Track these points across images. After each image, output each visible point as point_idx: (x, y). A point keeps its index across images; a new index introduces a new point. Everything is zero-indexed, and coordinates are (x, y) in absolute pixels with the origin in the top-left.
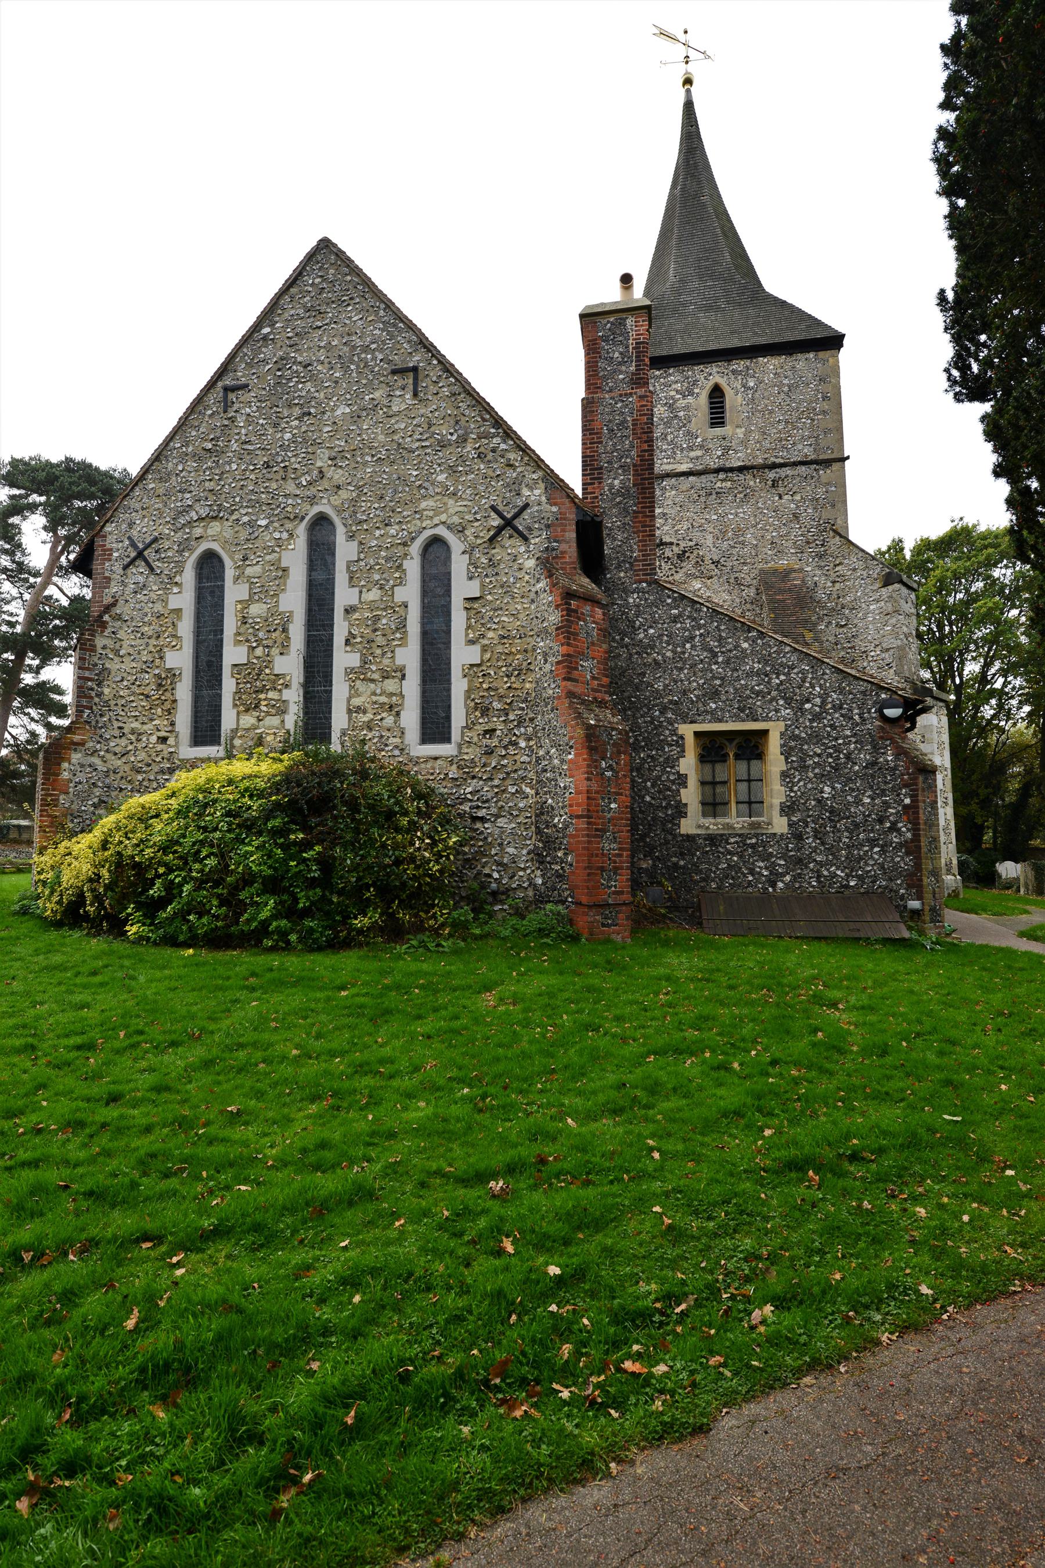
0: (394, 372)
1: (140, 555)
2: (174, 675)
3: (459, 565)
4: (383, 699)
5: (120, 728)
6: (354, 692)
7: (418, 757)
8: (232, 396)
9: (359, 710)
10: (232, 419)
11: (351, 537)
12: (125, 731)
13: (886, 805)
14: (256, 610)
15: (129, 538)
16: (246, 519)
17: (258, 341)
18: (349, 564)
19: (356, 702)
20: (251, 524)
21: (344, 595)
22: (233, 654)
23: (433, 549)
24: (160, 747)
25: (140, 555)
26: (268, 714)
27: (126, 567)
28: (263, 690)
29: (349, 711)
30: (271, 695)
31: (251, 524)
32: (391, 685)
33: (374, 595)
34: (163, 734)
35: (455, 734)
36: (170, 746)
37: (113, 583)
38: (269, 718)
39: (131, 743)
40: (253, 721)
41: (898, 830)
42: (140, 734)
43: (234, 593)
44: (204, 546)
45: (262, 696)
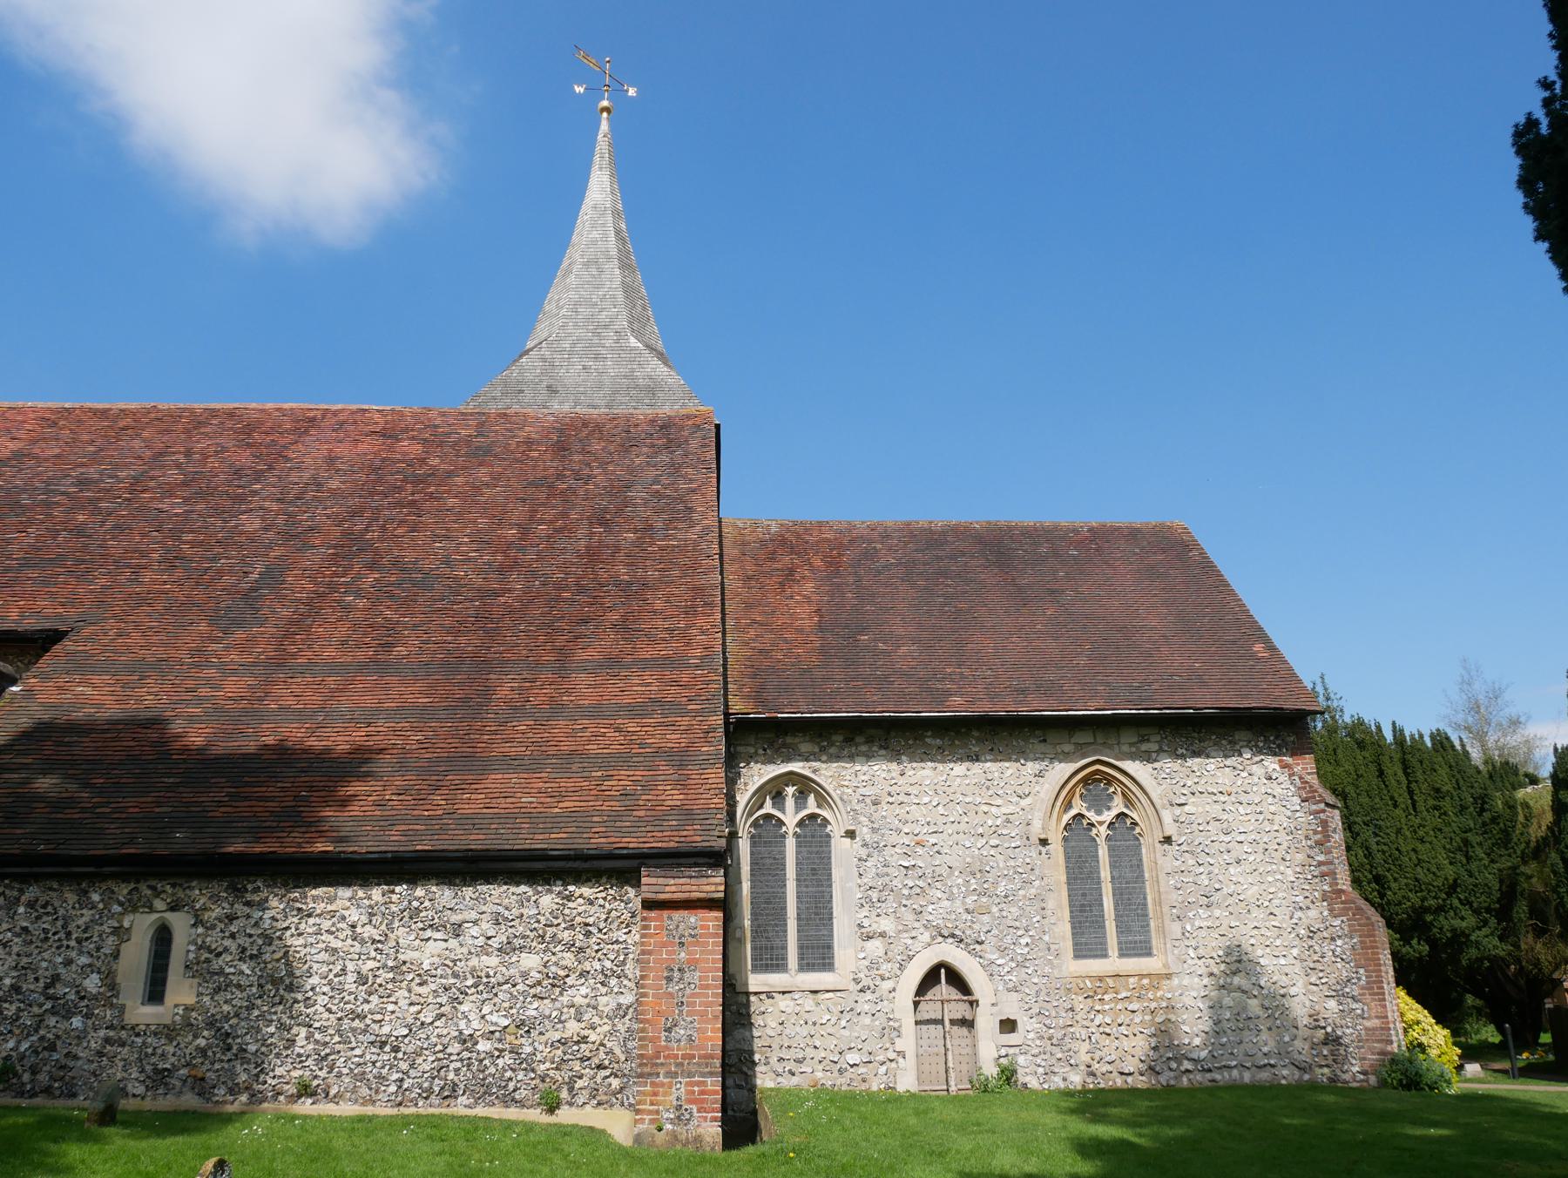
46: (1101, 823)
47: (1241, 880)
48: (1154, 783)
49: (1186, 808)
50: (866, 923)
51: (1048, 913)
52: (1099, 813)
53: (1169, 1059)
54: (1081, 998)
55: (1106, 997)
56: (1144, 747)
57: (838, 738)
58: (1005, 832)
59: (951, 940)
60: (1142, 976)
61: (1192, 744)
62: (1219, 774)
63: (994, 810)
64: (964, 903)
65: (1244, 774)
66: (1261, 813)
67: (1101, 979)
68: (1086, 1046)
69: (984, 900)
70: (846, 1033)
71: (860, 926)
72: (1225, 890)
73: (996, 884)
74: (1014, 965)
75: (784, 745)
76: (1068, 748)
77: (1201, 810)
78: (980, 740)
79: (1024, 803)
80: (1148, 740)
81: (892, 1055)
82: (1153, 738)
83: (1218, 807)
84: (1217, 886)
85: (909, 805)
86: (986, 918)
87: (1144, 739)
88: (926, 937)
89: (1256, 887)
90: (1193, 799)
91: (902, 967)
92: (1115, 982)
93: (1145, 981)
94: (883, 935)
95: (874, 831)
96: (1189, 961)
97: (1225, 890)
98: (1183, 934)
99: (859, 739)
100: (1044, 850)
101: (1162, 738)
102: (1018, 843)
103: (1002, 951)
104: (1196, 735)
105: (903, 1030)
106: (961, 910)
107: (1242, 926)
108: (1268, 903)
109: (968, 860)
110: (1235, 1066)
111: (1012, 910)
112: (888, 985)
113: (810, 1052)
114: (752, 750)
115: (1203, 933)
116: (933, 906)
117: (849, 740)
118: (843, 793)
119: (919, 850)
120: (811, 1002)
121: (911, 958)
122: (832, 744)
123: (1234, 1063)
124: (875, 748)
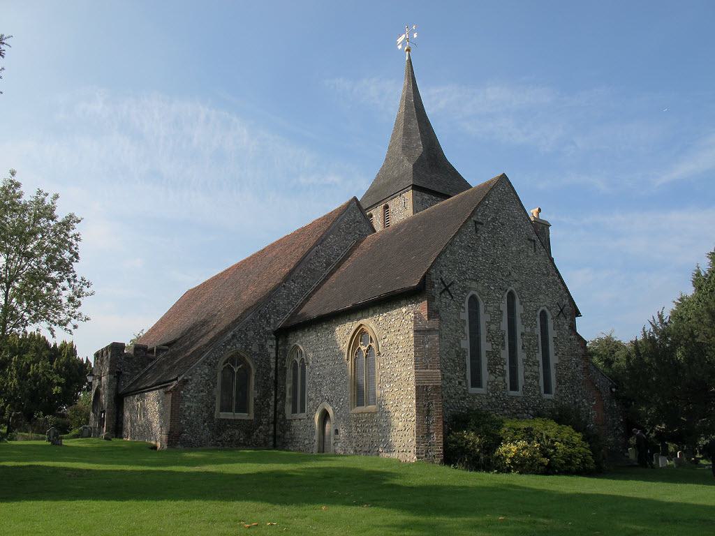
0: (529, 240)
1: (446, 289)
2: (465, 352)
3: (550, 324)
4: (534, 374)
6: (525, 371)
10: (479, 238)
11: (521, 304)
12: (445, 377)
13: (614, 421)
14: (493, 327)
15: (441, 279)
16: (486, 284)
18: (521, 314)
19: (527, 374)
20: (489, 287)
21: (520, 328)
22: (485, 346)
23: (543, 314)
24: (460, 387)
25: (446, 289)
27: (441, 294)
28: (496, 364)
30: (500, 367)
31: (489, 287)
32: (535, 368)
33: (528, 329)
34: (460, 380)
35: (553, 390)
37: (436, 300)
40: (494, 378)
41: (619, 430)
43: (484, 319)
44: (472, 292)
45: (497, 367)
49: (386, 340)
57: (306, 330)
60: (369, 413)
67: (358, 414)
72: (395, 375)
97: (395, 375)
104: (389, 306)
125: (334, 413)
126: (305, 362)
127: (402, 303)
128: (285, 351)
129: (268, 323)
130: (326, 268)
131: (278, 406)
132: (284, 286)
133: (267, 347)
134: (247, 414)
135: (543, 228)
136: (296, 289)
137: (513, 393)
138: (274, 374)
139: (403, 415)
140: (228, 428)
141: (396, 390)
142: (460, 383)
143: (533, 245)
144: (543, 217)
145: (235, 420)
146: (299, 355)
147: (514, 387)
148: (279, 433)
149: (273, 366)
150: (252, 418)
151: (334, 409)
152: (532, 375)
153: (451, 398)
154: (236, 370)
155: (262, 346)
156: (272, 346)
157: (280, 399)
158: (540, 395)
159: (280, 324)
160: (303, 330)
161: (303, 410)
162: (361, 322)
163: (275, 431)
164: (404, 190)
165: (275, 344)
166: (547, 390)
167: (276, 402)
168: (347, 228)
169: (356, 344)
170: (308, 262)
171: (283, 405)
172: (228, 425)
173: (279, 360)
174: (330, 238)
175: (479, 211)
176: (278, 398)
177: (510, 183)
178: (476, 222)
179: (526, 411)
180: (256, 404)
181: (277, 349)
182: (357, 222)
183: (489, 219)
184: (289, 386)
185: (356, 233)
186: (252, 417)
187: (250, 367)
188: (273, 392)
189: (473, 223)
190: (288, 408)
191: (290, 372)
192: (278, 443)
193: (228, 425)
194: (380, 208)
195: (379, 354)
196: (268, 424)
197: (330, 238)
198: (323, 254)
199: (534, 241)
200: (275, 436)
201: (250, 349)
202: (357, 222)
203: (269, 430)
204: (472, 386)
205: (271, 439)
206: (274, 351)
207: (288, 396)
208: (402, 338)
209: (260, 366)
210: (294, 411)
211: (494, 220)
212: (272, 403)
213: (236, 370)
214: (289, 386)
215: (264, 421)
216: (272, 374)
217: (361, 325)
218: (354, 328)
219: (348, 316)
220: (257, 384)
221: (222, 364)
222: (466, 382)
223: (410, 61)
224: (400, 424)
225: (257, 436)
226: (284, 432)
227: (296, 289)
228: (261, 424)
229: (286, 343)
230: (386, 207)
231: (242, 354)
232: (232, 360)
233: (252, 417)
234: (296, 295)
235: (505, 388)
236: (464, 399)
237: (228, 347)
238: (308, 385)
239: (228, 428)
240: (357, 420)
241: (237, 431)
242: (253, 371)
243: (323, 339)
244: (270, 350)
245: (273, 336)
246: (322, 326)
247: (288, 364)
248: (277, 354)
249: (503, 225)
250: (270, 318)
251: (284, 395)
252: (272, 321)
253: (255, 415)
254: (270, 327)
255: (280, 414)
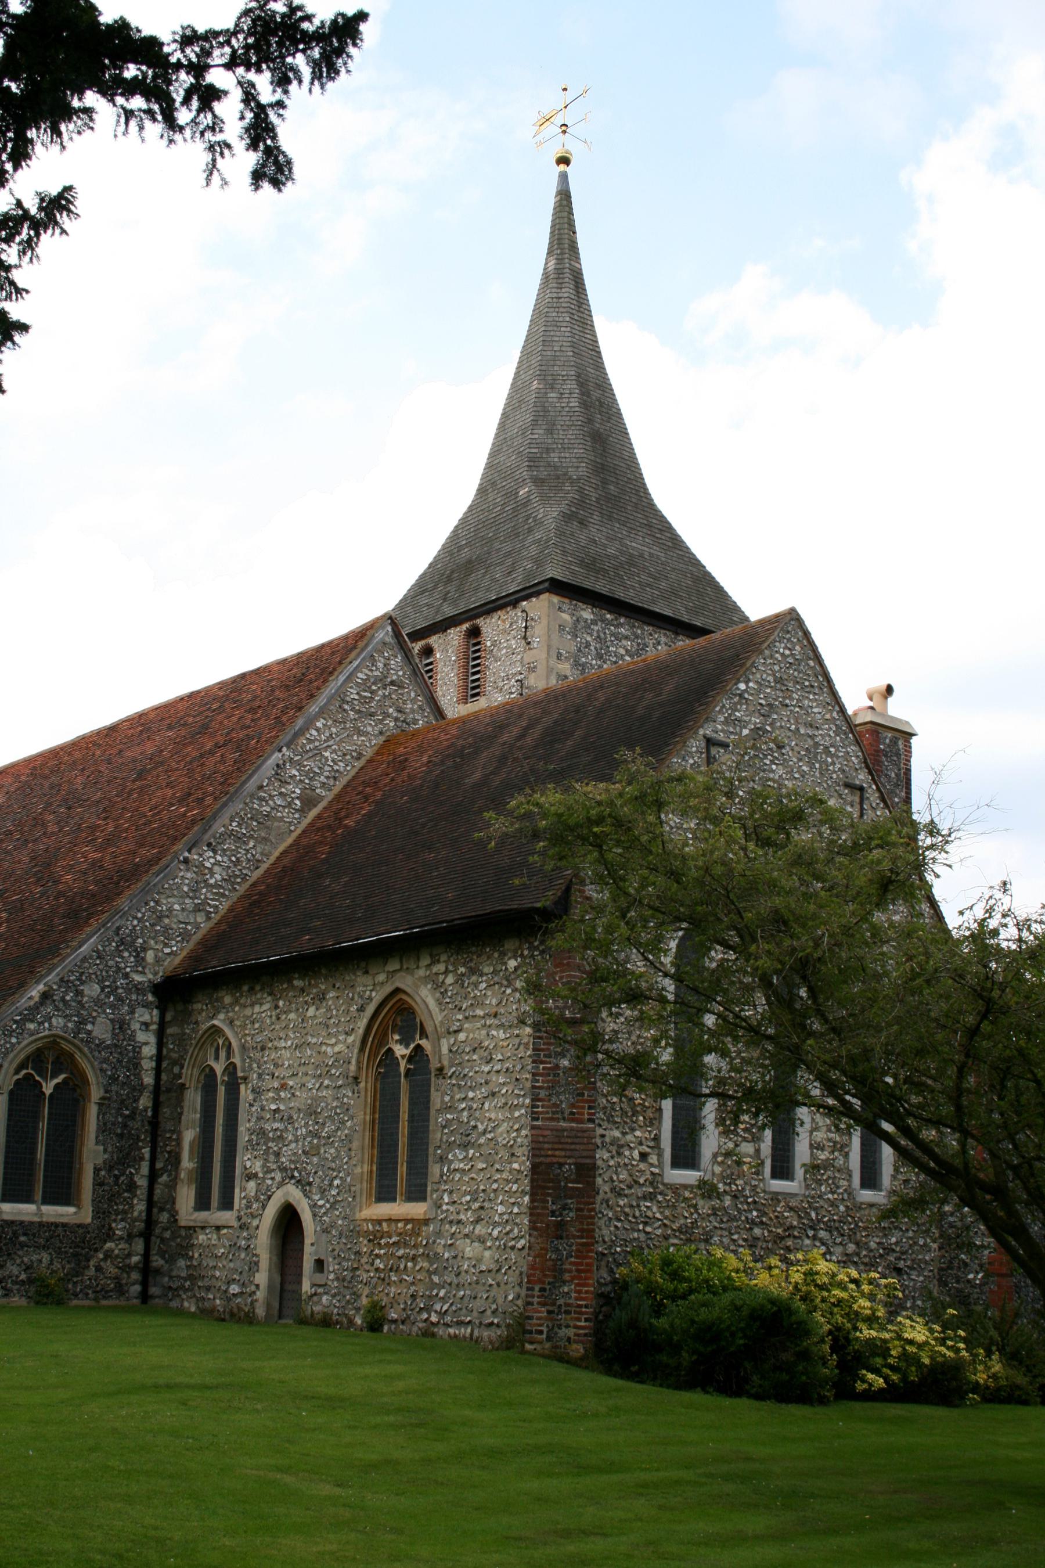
0: (847, 785)
5: (603, 1136)
7: (862, 1203)
8: (714, 751)
9: (820, 1147)
17: (735, 695)
24: (642, 1166)
26: (745, 1139)
29: (811, 1146)
35: (886, 1180)
36: (652, 1165)
38: (744, 1144)
39: (612, 1157)
42: (622, 1146)
46: (403, 1057)
47: (493, 1116)
48: (437, 1010)
49: (462, 1036)
50: (248, 1164)
51: (353, 1154)
52: (407, 1046)
53: (421, 1309)
54: (365, 1242)
55: (383, 1242)
56: (435, 969)
57: (245, 988)
58: (333, 1071)
59: (293, 1181)
60: (407, 1221)
61: (471, 960)
62: (489, 993)
63: (329, 1050)
64: (303, 1144)
65: (509, 991)
66: (518, 1036)
67: (379, 1222)
68: (366, 1291)
69: (315, 1141)
70: (232, 1265)
71: (246, 1169)
72: (481, 1127)
73: (324, 1124)
74: (328, 1206)
75: (217, 1000)
76: (382, 977)
77: (471, 1036)
78: (326, 978)
79: (350, 1039)
80: (439, 961)
81: (253, 1288)
82: (444, 958)
83: (484, 1032)
84: (473, 1123)
85: (281, 1049)
86: (315, 1160)
87: (435, 961)
88: (278, 1176)
89: (505, 1124)
90: (466, 1026)
91: (264, 1207)
92: (389, 1226)
93: (409, 1226)
94: (256, 1176)
95: (260, 1076)
96: (445, 1207)
97: (481, 1127)
98: (442, 1176)
99: (258, 988)
100: (356, 1088)
101: (449, 957)
102: (340, 1083)
103: (323, 1192)
104: (474, 949)
105: (260, 1264)
106: (300, 1152)
107: (489, 1168)
108: (512, 1142)
109: (309, 1101)
110: (470, 1322)
111: (333, 1151)
112: (255, 1223)
113: (214, 1282)
114: (199, 1006)
115: (457, 1176)
116: (285, 1149)
117: (252, 989)
118: (246, 1041)
119: (282, 1094)
120: (215, 1236)
121: (269, 1197)
122: (242, 996)
123: (469, 1319)
124: (265, 995)
125: (314, 1215)
126: (240, 1074)
127: (510, 945)
128: (182, 1040)
129: (140, 960)
130: (302, 811)
131: (158, 1191)
132: (186, 861)
133: (135, 1026)
134: (72, 1210)
135: (894, 742)
136: (216, 869)
137: (778, 1185)
138: (150, 1104)
139: (495, 1233)
140: (23, 1245)
141: (481, 1165)
142: (644, 1156)
143: (857, 799)
144: (897, 709)
145: (41, 1224)
146: (223, 1054)
147: (782, 1169)
148: (157, 1261)
149: (148, 1080)
150: (89, 1220)
151: (314, 1206)
152: (829, 1140)
153: (620, 1194)
154: (48, 1088)
155: (121, 1026)
156: (146, 1025)
157: (164, 1170)
158: (849, 1191)
159: (170, 965)
160: (238, 987)
161: (227, 1203)
162: (404, 982)
163: (146, 1255)
164: (528, 593)
165: (156, 1019)
166: (870, 1179)
167: (153, 1176)
168: (364, 701)
169: (382, 1038)
170: (252, 796)
171: (172, 1185)
172: (22, 1239)
173: (164, 1065)
174: (318, 730)
175: (720, 712)
176: (159, 1165)
177: (807, 634)
178: (710, 742)
179: (811, 1233)
180: (98, 1183)
181: (161, 1035)
182: (392, 683)
183: (745, 732)
184: (189, 1136)
185: (387, 715)
186: (86, 1216)
187: (86, 1081)
188: (146, 1152)
189: (703, 744)
190: (186, 1197)
191: (193, 1099)
192: (153, 1290)
193: (22, 1239)
194: (455, 636)
195: (441, 1070)
196: (130, 1237)
197: (318, 730)
198: (295, 772)
199: (861, 789)
200: (147, 1271)
201: (89, 1033)
202: (392, 683)
203: (129, 1255)
204: (676, 1164)
205: (135, 1276)
206: (152, 1039)
207: (187, 1163)
208: (502, 1035)
209: (114, 1079)
210: (203, 1203)
211: (758, 732)
212: (142, 1182)
213: (48, 1088)
214: (189, 1136)
215: (119, 1229)
216: (145, 1102)
217: (397, 990)
218: (377, 997)
219: (363, 964)
220: (103, 1128)
221: (12, 1071)
222: (660, 1155)
223: (564, 199)
224: (487, 1254)
225: (98, 1269)
226: (171, 1260)
227: (216, 869)
228: (109, 1236)
229: (184, 1018)
230: (475, 633)
231: (64, 1045)
232: (36, 1059)
233: (86, 1216)
234: (216, 886)
235: (757, 1173)
236: (651, 1197)
237: (31, 1026)
238: (243, 1136)
239: (23, 1245)
240: (374, 1238)
241: (45, 1257)
242: (96, 1093)
243: (292, 1016)
244: (141, 1037)
245: (150, 998)
246: (290, 982)
247: (190, 1075)
248: (160, 1045)
249: (780, 747)
250: (145, 950)
251: (175, 1159)
252: (150, 956)
253: (97, 1213)
254: (143, 973)
255: (162, 1210)
